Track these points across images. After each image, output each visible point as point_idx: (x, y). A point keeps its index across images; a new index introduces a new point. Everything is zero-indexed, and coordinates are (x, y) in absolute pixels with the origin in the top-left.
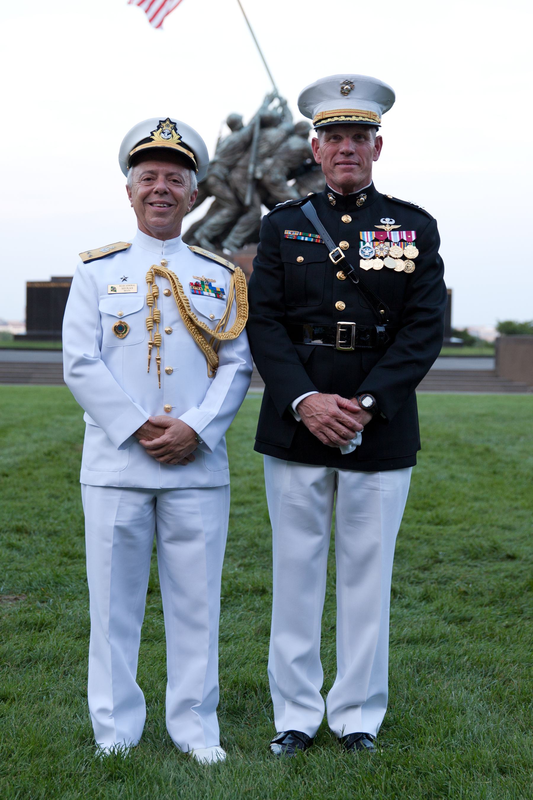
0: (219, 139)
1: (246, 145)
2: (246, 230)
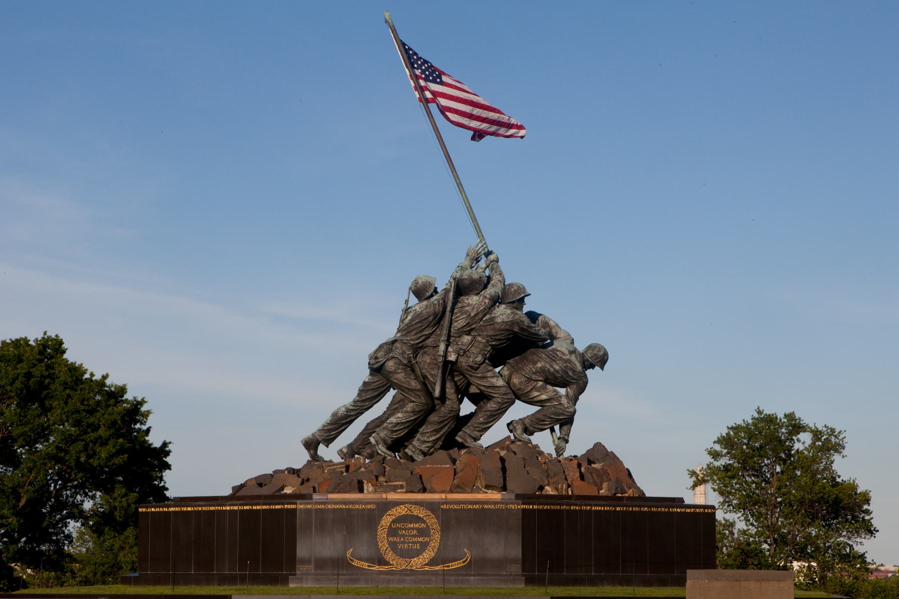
0: (406, 311)
1: (438, 318)
2: (437, 431)
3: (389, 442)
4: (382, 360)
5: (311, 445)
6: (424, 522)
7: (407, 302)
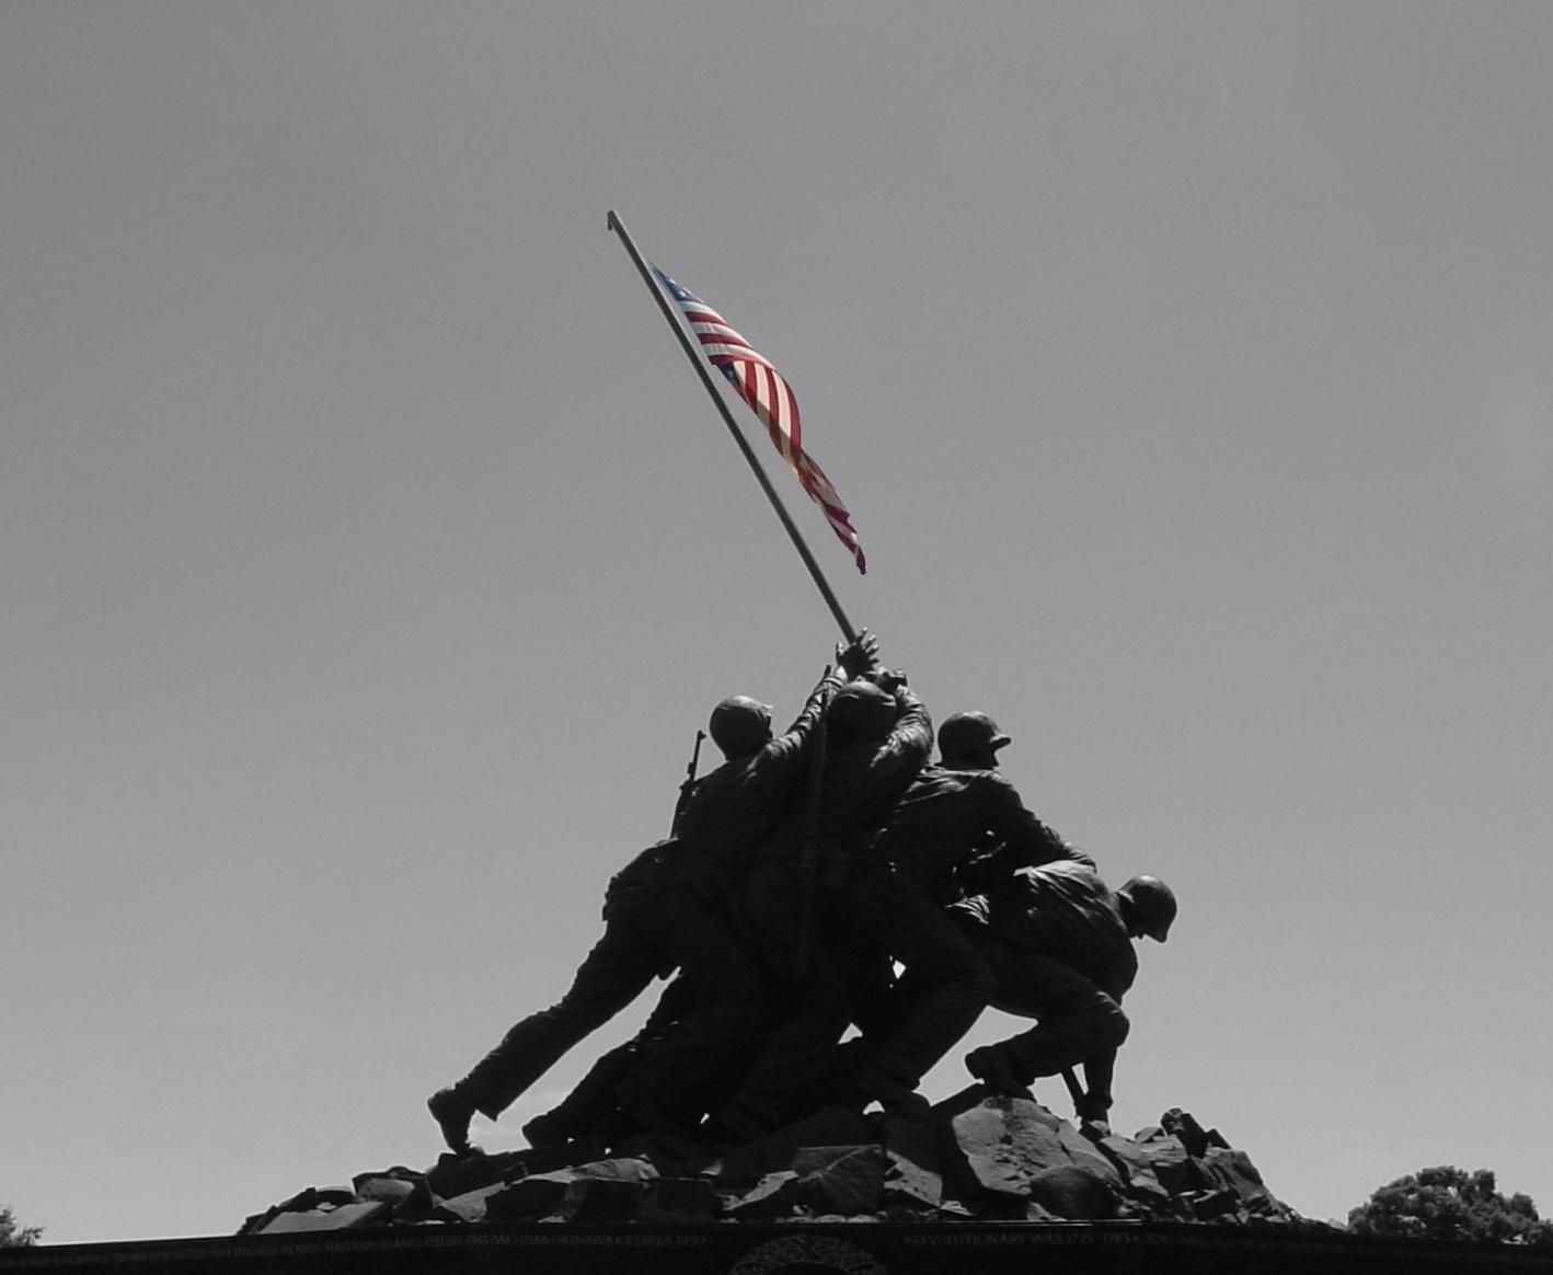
5: (452, 1110)
7: (692, 768)
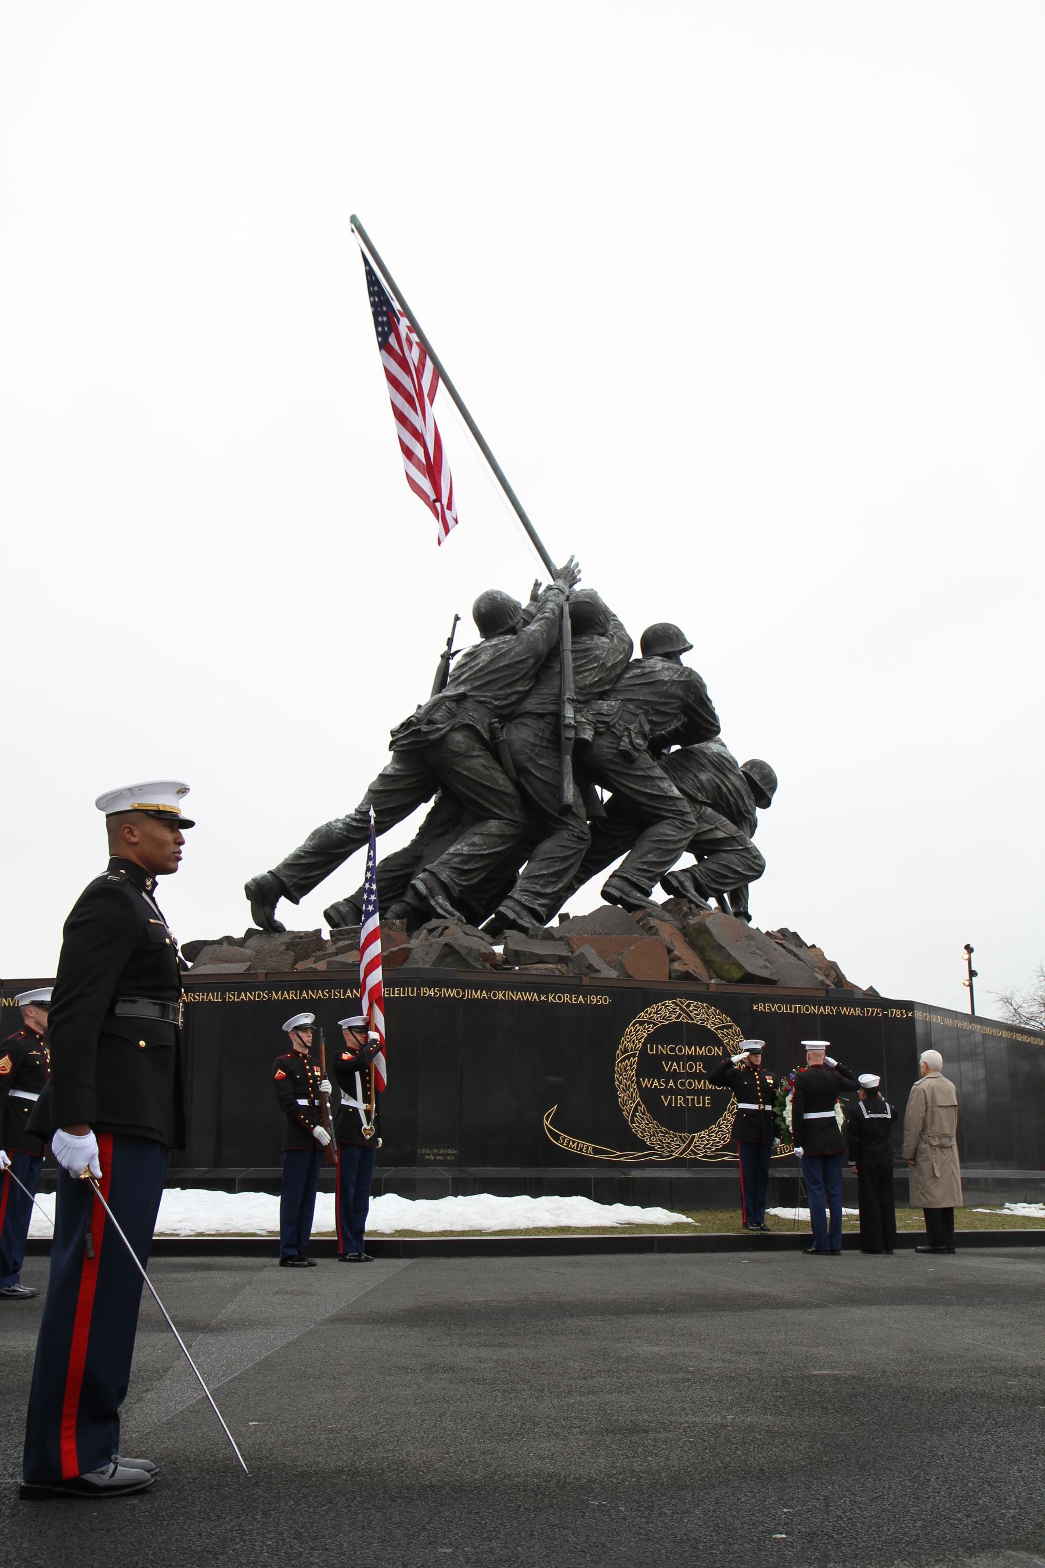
0: (447, 657)
3: (456, 892)
4: (444, 727)
6: (719, 1043)
7: (450, 642)
